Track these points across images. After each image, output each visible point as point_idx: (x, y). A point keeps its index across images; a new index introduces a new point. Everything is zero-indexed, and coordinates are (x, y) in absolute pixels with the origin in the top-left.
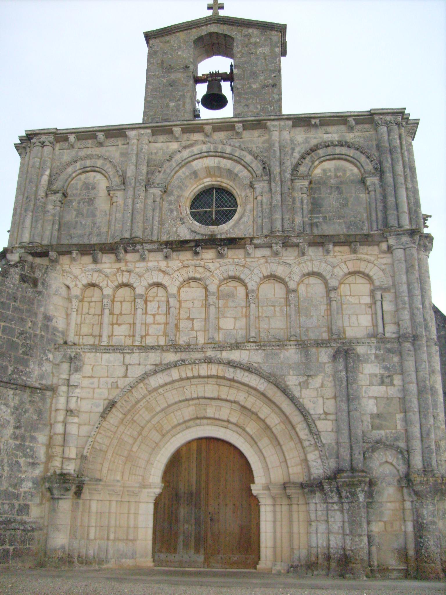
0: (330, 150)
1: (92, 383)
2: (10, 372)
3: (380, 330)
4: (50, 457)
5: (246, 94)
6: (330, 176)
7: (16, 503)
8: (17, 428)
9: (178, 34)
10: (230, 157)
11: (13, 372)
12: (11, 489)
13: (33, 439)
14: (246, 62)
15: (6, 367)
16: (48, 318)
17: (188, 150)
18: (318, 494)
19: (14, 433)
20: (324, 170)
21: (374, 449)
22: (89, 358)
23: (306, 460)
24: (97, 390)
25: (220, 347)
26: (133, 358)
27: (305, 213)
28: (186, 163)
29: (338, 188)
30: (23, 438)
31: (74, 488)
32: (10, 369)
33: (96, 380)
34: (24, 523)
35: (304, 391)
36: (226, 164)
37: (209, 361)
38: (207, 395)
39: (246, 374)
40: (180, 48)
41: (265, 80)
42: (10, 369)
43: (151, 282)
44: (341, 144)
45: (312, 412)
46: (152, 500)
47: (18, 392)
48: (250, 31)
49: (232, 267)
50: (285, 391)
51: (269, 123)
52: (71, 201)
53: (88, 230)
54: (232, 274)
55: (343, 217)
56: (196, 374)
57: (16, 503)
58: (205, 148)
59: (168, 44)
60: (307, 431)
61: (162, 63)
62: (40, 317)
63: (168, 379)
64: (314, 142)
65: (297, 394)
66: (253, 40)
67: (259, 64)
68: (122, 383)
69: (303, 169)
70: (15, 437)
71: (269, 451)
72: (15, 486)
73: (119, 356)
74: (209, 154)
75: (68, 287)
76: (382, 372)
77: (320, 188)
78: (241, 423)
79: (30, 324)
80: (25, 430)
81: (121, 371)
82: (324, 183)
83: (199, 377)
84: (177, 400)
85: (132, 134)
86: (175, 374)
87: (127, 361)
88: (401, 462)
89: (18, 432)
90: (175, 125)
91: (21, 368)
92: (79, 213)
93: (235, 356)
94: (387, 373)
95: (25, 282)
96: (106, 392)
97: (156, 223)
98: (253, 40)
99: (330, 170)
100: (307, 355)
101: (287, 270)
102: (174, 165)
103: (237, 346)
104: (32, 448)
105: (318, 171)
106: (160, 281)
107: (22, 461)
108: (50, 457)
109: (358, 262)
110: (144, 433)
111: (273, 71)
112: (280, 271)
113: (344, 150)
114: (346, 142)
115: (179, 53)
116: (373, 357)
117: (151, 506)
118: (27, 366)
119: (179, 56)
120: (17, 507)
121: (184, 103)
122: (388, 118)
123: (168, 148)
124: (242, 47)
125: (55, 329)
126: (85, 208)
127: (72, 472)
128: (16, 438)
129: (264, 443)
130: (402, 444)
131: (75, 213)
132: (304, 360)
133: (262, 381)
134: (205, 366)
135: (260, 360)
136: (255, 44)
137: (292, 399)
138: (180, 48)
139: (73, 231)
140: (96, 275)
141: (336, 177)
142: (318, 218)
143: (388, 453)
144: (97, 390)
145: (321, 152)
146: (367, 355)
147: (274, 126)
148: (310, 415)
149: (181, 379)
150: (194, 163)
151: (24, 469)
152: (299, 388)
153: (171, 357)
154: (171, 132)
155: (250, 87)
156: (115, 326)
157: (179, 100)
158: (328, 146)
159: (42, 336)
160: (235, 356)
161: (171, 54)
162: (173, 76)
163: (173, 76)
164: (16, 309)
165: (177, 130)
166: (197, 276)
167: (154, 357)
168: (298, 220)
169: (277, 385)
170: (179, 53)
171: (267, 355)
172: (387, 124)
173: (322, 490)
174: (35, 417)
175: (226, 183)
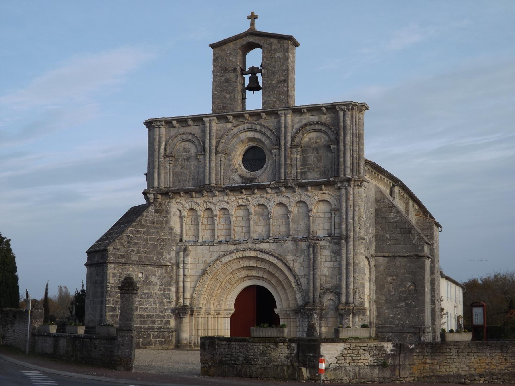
0: (312, 127)
1: (195, 261)
2: (155, 259)
3: (333, 232)
4: (178, 298)
5: (269, 87)
6: (313, 142)
7: (164, 320)
8: (160, 285)
9: (229, 44)
10: (259, 131)
11: (156, 259)
12: (160, 314)
13: (169, 290)
14: (269, 64)
15: (153, 257)
16: (171, 229)
17: (237, 128)
18: (299, 313)
19: (160, 288)
20: (310, 139)
21: (324, 293)
22: (192, 249)
23: (296, 298)
24: (198, 265)
25: (255, 241)
26: (213, 248)
27: (298, 166)
28: (236, 135)
29: (317, 150)
30: (164, 290)
31: (189, 312)
32: (155, 258)
33: (197, 260)
34: (169, 328)
35: (295, 264)
36: (258, 136)
37: (250, 250)
38: (251, 265)
39: (268, 255)
40: (231, 54)
41: (280, 77)
42: (155, 258)
43: (221, 208)
44: (318, 123)
45: (298, 274)
46: (230, 317)
47: (160, 268)
48: (272, 40)
49: (260, 199)
50: (285, 264)
51: (279, 112)
52: (177, 160)
53: (188, 177)
54: (260, 203)
55: (319, 168)
56: (244, 256)
57: (164, 320)
58: (246, 126)
59: (224, 52)
60: (296, 284)
62: (167, 229)
63: (230, 259)
64: (304, 121)
65: (292, 265)
66: (273, 47)
67: (276, 65)
68: (209, 260)
69: (297, 140)
70: (160, 290)
71: (281, 293)
72: (162, 312)
73: (207, 247)
74: (249, 130)
75: (180, 211)
76: (332, 254)
77: (307, 150)
78: (269, 278)
79: (162, 234)
80: (165, 286)
81: (208, 255)
82: (310, 147)
83: (246, 257)
84: (237, 268)
85: (206, 120)
86: (234, 256)
87: (211, 250)
88: (337, 299)
89: (161, 287)
90: (229, 115)
91: (160, 257)
92: (182, 167)
93: (263, 246)
94: (334, 255)
95: (157, 213)
96: (202, 266)
97: (222, 174)
98: (273, 47)
99: (313, 139)
100: (297, 245)
101: (288, 200)
102: (230, 137)
103: (263, 241)
104: (169, 294)
105: (306, 139)
106: (225, 207)
107: (165, 301)
108: (178, 298)
109: (324, 195)
110: (223, 284)
111: (284, 71)
112: (284, 200)
113: (320, 127)
114: (321, 122)
115: (231, 59)
116: (328, 247)
117: (229, 319)
118: (163, 255)
119: (230, 60)
120: (164, 321)
121: (235, 95)
122: (343, 107)
123: (226, 126)
124: (267, 53)
125: (175, 234)
126: (185, 163)
127: (188, 305)
128: (161, 290)
129: (279, 289)
130: (338, 290)
131: (180, 167)
132: (295, 248)
133: (275, 259)
134: (248, 252)
135: (274, 248)
136: (275, 49)
137: (289, 268)
138: (231, 54)
139: (180, 178)
140: (193, 204)
141: (316, 142)
142: (305, 168)
143: (331, 295)
144: (198, 265)
145: (307, 128)
146: (325, 246)
147: (281, 114)
148: (298, 276)
149: (237, 258)
150: (241, 135)
151: (166, 304)
152: (292, 263)
153: (232, 247)
154: (227, 118)
155: (271, 83)
156: (205, 231)
157: (232, 93)
158: (311, 124)
159: (169, 239)
160: (263, 246)
161: (226, 60)
162: (227, 76)
163: (227, 76)
164: (154, 227)
165: (230, 118)
166: (244, 204)
167: (224, 248)
168: (294, 171)
169: (282, 261)
170: (231, 59)
171: (278, 246)
172: (344, 111)
173: (301, 312)
174: (169, 279)
175: (260, 145)
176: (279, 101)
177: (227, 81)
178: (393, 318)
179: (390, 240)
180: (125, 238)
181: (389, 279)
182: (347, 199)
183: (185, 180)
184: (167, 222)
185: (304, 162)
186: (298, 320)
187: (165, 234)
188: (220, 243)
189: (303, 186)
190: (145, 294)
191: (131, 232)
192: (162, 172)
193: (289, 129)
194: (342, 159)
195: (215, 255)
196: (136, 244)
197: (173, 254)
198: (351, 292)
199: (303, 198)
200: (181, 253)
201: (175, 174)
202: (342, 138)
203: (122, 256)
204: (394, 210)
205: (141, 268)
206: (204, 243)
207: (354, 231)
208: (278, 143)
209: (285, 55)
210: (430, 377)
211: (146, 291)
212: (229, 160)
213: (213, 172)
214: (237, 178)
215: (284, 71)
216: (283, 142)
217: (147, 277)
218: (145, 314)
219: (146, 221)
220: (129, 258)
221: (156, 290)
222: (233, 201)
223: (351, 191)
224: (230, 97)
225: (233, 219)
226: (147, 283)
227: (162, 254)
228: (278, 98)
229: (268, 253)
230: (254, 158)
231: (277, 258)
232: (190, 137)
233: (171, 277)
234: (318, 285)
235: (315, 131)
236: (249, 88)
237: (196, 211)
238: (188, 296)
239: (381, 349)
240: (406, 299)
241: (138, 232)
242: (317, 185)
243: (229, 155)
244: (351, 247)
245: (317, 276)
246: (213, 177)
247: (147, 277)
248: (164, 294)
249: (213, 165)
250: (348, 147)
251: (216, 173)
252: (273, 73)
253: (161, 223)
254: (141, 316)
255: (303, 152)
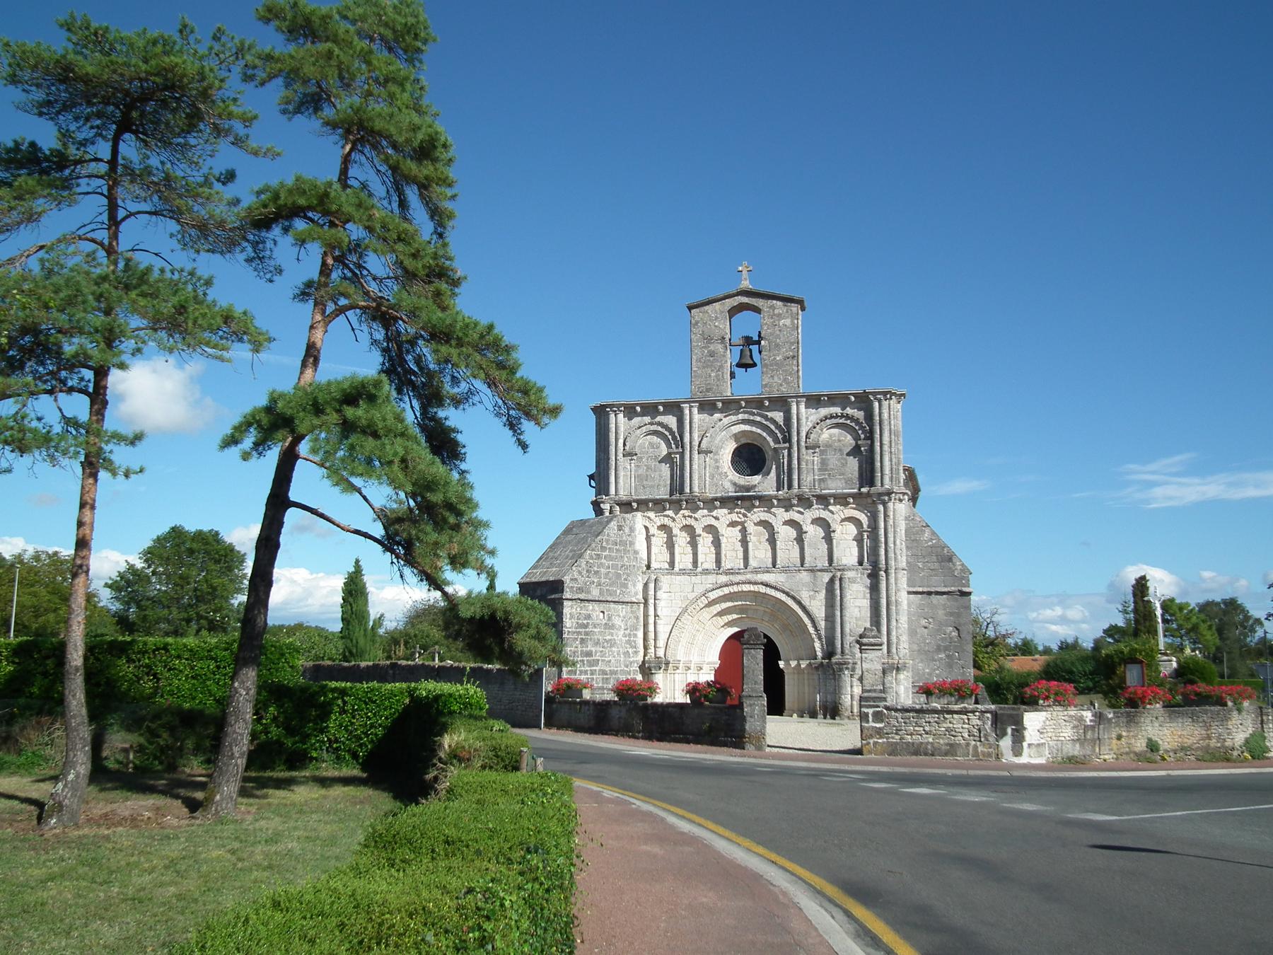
13: (635, 636)
14: (771, 334)
16: (636, 552)
22: (665, 581)
25: (756, 571)
37: (750, 583)
44: (842, 416)
50: (799, 603)
61: (703, 334)
68: (692, 596)
74: (744, 422)
92: (648, 468)
108: (646, 648)
111: (792, 344)
112: (797, 517)
136: (780, 315)
138: (716, 318)
153: (723, 579)
163: (712, 347)
167: (711, 579)
168: (810, 478)
172: (880, 401)
176: (788, 383)
177: (712, 354)
178: (930, 674)
179: (923, 570)
180: (583, 565)
181: (924, 622)
182: (886, 516)
183: (652, 487)
184: (632, 543)
185: (824, 465)
186: (816, 677)
187: (629, 558)
188: (706, 572)
189: (823, 500)
190: (607, 641)
191: (591, 557)
192: (621, 474)
193: (803, 421)
194: (878, 464)
195: (700, 590)
196: (596, 573)
197: (640, 587)
198: (894, 639)
199: (824, 514)
200: (652, 586)
201: (638, 477)
202: (877, 436)
203: (580, 590)
204: (927, 530)
205: (602, 606)
206: (683, 572)
207: (896, 559)
208: (787, 439)
209: (792, 323)
210: (1127, 753)
211: (608, 638)
212: (717, 461)
213: (696, 476)
214: (728, 485)
215: (792, 344)
216: (795, 439)
217: (609, 619)
218: (607, 669)
219: (607, 541)
220: (589, 592)
221: (619, 636)
222: (723, 516)
223: (890, 505)
224: (717, 376)
225: (723, 540)
226: (609, 626)
227: (625, 586)
228: (785, 380)
229: (775, 588)
230: (750, 457)
231: (787, 594)
232: (659, 429)
233: (637, 618)
234: (847, 630)
235: (837, 426)
236: (739, 365)
237: (671, 529)
238: (661, 643)
239: (1081, 719)
240: (946, 649)
241: (599, 557)
242: (842, 500)
243: (717, 454)
244: (892, 580)
245: (846, 619)
246: (696, 482)
247: (609, 619)
248: (629, 642)
249: (695, 467)
250: (886, 448)
251: (700, 477)
252: (777, 345)
253: (623, 543)
254: (604, 672)
255: (822, 453)
